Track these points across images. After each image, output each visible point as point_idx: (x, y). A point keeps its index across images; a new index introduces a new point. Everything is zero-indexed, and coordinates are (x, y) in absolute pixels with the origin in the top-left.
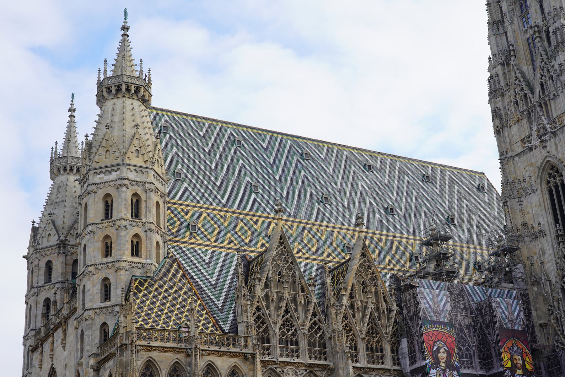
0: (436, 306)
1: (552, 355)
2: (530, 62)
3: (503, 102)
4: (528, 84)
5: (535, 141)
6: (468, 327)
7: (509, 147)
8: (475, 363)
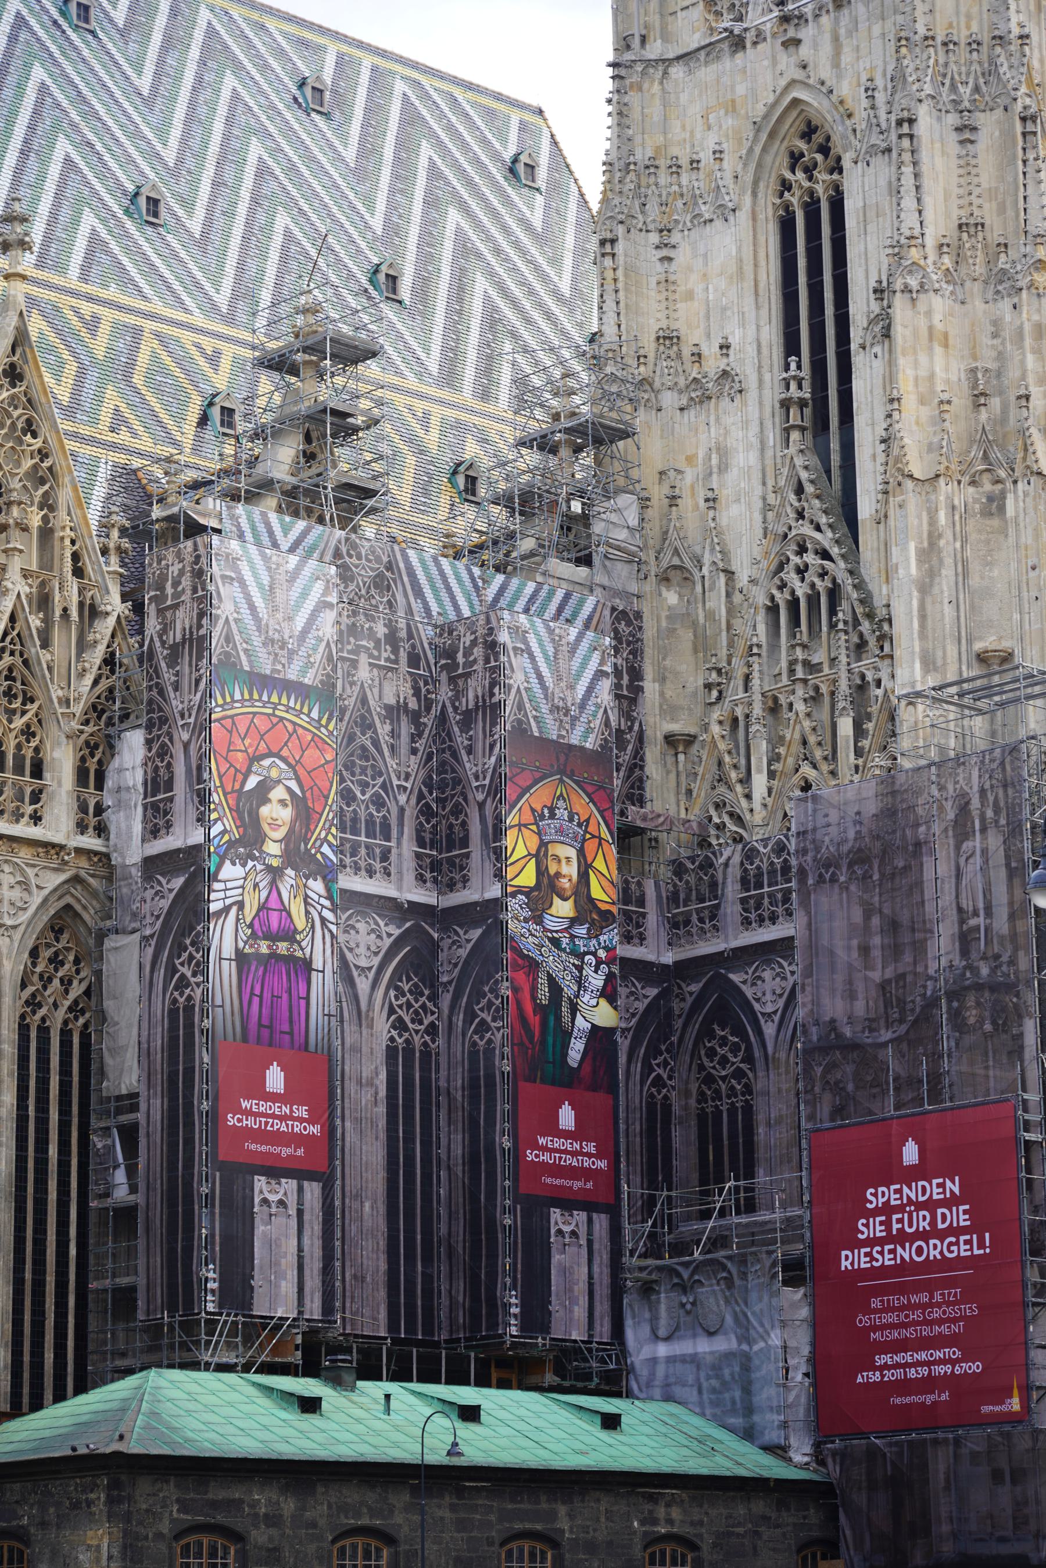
0: (279, 616)
1: (692, 859)
6: (393, 712)
7: (655, 19)
8: (400, 855)
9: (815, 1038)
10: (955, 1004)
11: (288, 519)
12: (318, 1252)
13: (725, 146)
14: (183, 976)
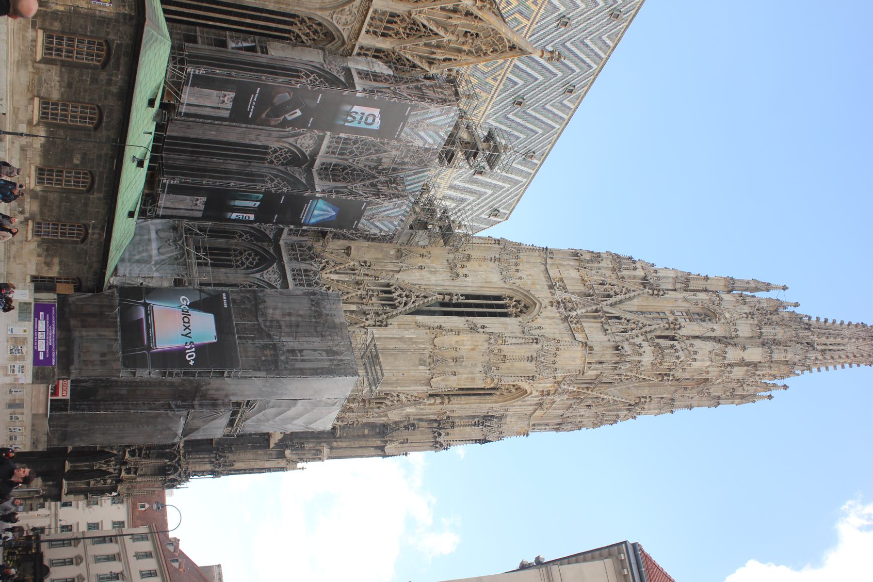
0: (426, 127)
2: (640, 310)
3: (606, 268)
4: (621, 302)
5: (559, 295)
6: (379, 161)
7: (557, 262)
8: (332, 158)
9: (259, 294)
10: (271, 347)
11: (449, 133)
12: (203, 113)
13: (522, 281)
14: (310, 76)
